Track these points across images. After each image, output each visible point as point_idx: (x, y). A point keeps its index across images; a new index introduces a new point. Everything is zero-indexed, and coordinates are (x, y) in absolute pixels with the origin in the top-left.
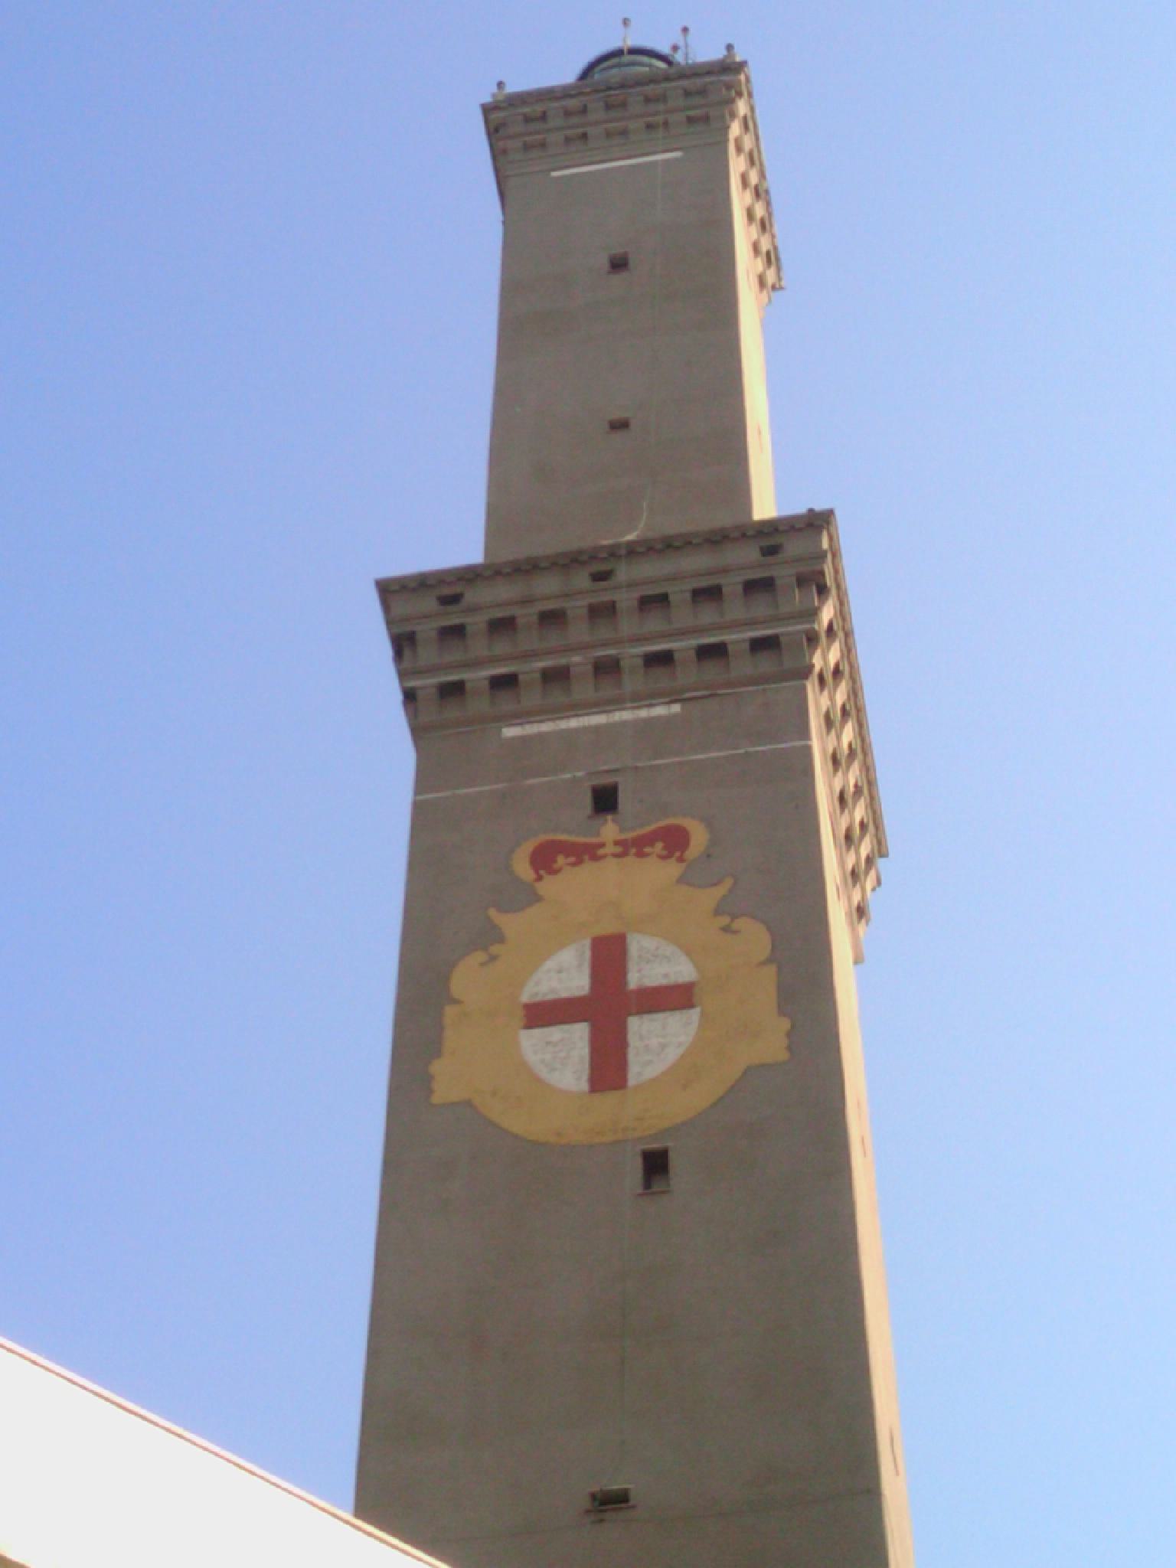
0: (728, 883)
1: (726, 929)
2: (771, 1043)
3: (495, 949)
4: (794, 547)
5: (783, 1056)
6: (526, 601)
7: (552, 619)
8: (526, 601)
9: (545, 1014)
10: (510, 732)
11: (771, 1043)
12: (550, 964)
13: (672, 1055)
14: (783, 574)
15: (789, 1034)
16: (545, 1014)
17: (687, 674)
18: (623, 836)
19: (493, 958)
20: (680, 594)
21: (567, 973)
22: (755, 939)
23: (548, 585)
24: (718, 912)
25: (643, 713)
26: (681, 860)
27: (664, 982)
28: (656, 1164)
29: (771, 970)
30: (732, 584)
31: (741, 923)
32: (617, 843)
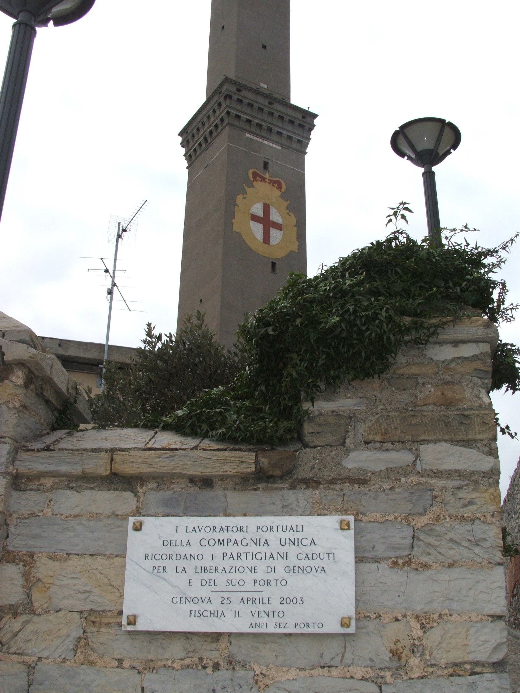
0: (289, 202)
1: (288, 214)
2: (294, 247)
3: (245, 195)
4: (308, 120)
5: (297, 251)
6: (257, 102)
7: (261, 110)
8: (257, 102)
9: (255, 218)
10: (248, 135)
11: (294, 247)
12: (255, 205)
13: (278, 241)
14: (307, 126)
15: (298, 246)
16: (255, 218)
17: (285, 141)
18: (271, 179)
19: (244, 198)
20: (287, 118)
21: (258, 210)
22: (293, 220)
23: (260, 100)
24: (287, 209)
25: (274, 146)
26: (280, 191)
27: (277, 221)
28: (274, 264)
29: (295, 228)
30: (297, 122)
31: (291, 213)
32: (269, 180)
